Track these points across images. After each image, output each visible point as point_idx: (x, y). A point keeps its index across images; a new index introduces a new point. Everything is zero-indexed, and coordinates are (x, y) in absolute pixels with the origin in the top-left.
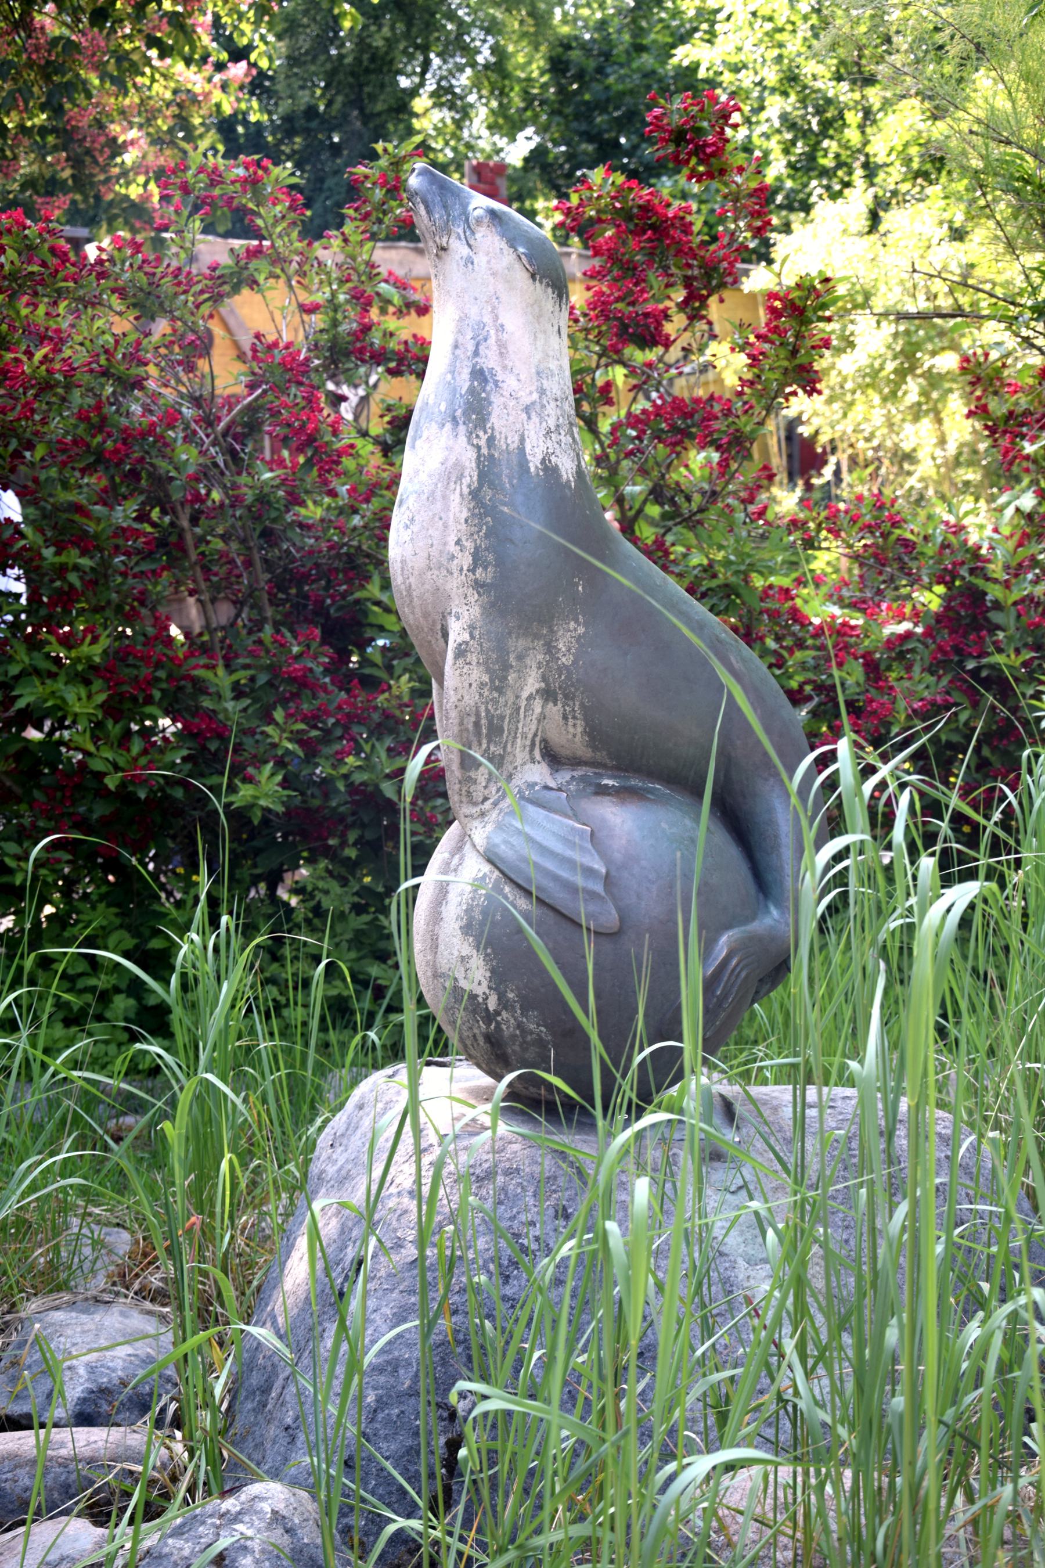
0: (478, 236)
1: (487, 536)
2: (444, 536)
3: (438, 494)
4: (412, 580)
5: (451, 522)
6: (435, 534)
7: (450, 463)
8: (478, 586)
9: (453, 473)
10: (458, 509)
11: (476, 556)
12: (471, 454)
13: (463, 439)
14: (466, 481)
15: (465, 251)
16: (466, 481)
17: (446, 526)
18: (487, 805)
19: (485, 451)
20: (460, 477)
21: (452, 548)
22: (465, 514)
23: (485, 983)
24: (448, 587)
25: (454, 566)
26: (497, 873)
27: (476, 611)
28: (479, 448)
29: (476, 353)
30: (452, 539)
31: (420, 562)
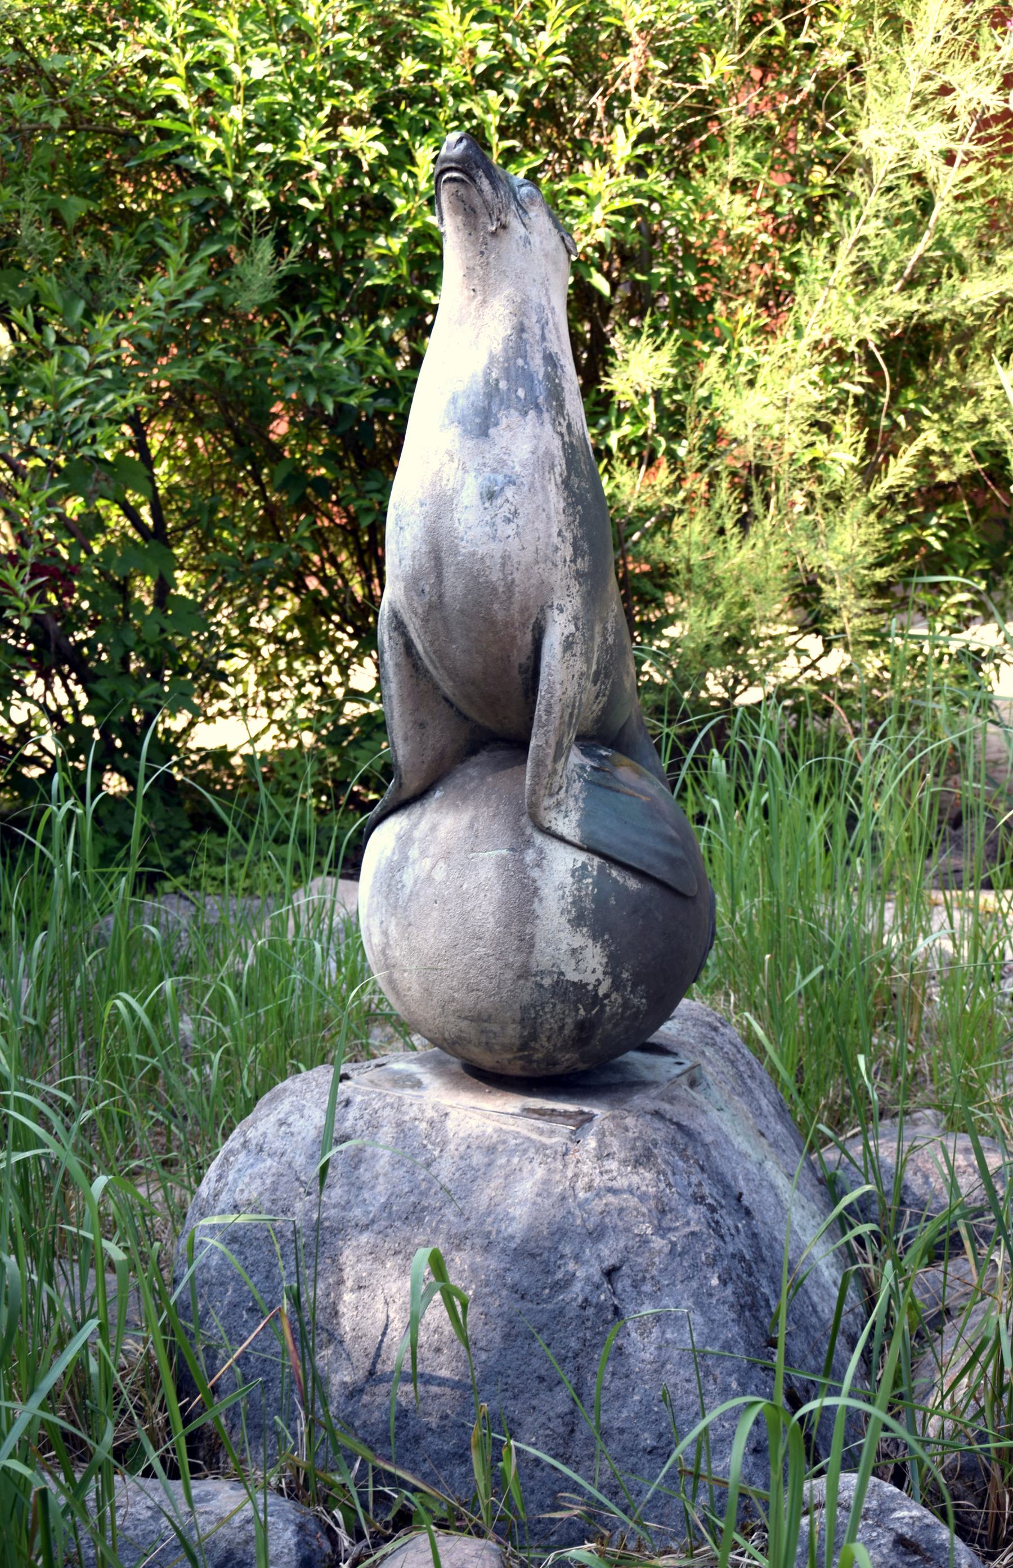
0: (532, 214)
1: (581, 525)
2: (548, 528)
3: (538, 484)
4: (517, 576)
5: (553, 513)
6: (541, 526)
7: (541, 452)
8: (579, 575)
9: (543, 463)
10: (556, 500)
11: (574, 545)
12: (557, 442)
13: (548, 427)
14: (558, 470)
15: (522, 231)
16: (558, 470)
17: (549, 518)
18: (562, 794)
19: (567, 438)
20: (552, 467)
21: (556, 540)
22: (562, 505)
23: (600, 970)
24: (552, 580)
25: (558, 558)
26: (597, 861)
27: (577, 601)
28: (562, 435)
29: (543, 338)
30: (555, 530)
31: (528, 557)
